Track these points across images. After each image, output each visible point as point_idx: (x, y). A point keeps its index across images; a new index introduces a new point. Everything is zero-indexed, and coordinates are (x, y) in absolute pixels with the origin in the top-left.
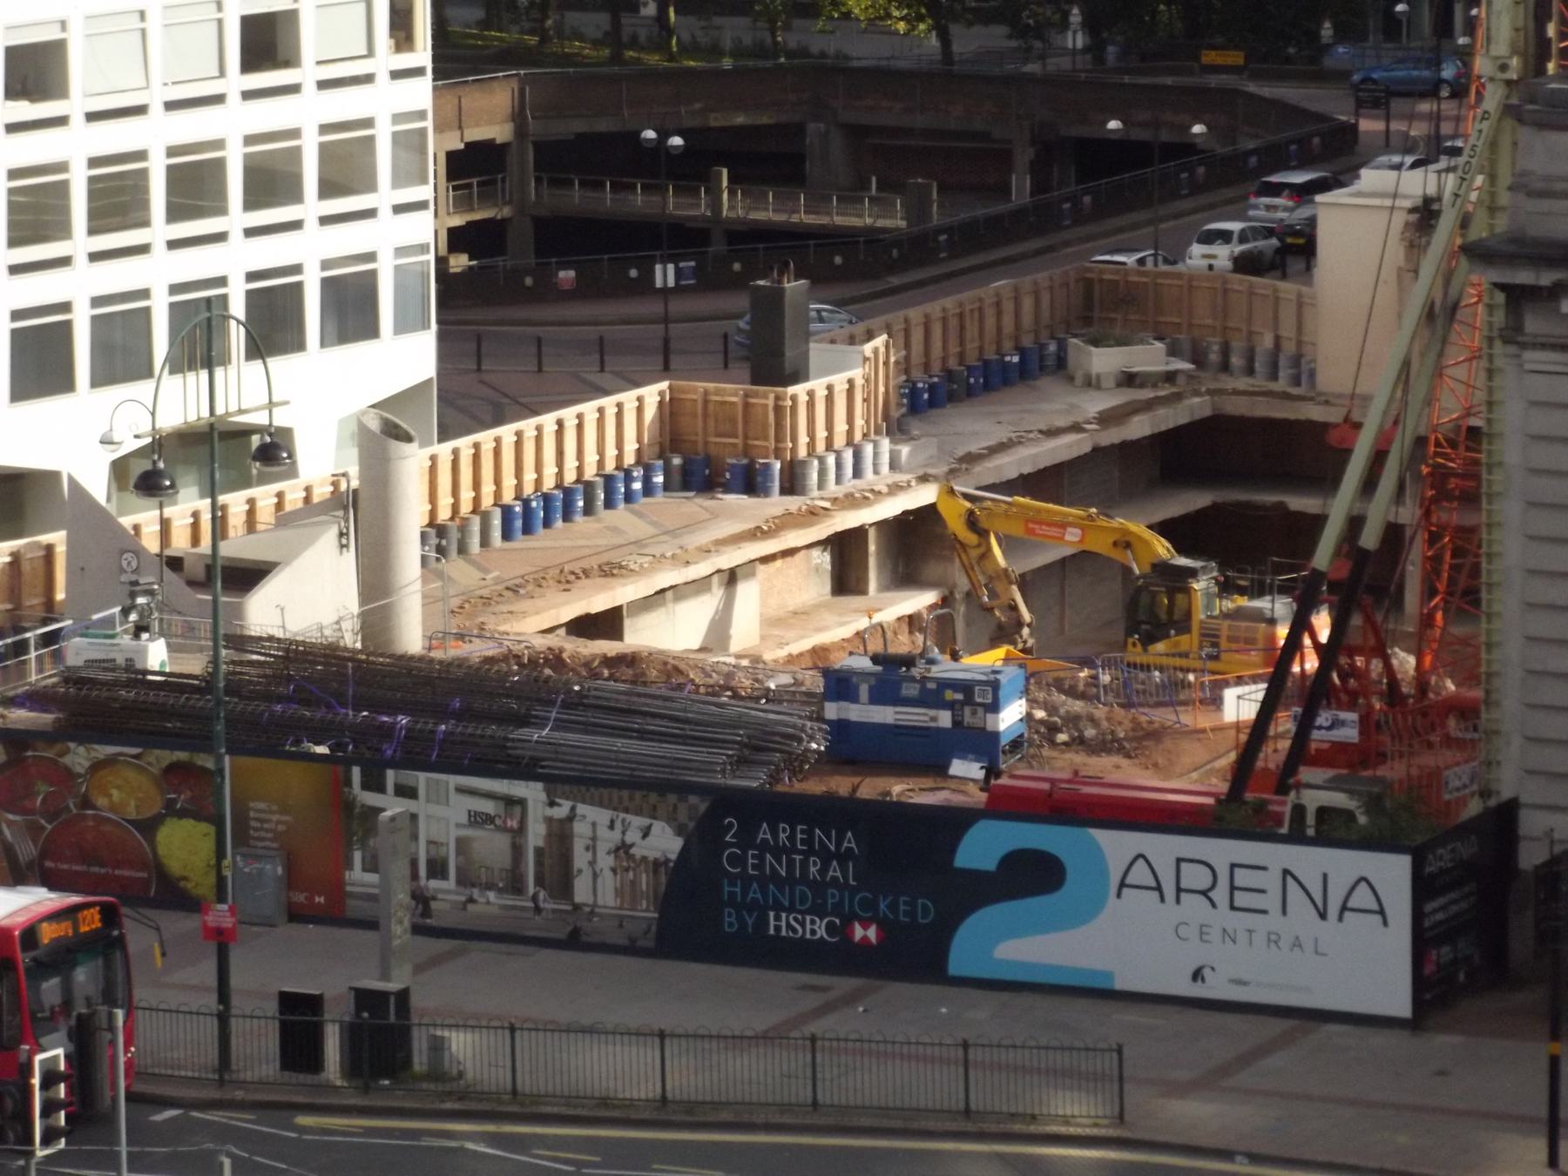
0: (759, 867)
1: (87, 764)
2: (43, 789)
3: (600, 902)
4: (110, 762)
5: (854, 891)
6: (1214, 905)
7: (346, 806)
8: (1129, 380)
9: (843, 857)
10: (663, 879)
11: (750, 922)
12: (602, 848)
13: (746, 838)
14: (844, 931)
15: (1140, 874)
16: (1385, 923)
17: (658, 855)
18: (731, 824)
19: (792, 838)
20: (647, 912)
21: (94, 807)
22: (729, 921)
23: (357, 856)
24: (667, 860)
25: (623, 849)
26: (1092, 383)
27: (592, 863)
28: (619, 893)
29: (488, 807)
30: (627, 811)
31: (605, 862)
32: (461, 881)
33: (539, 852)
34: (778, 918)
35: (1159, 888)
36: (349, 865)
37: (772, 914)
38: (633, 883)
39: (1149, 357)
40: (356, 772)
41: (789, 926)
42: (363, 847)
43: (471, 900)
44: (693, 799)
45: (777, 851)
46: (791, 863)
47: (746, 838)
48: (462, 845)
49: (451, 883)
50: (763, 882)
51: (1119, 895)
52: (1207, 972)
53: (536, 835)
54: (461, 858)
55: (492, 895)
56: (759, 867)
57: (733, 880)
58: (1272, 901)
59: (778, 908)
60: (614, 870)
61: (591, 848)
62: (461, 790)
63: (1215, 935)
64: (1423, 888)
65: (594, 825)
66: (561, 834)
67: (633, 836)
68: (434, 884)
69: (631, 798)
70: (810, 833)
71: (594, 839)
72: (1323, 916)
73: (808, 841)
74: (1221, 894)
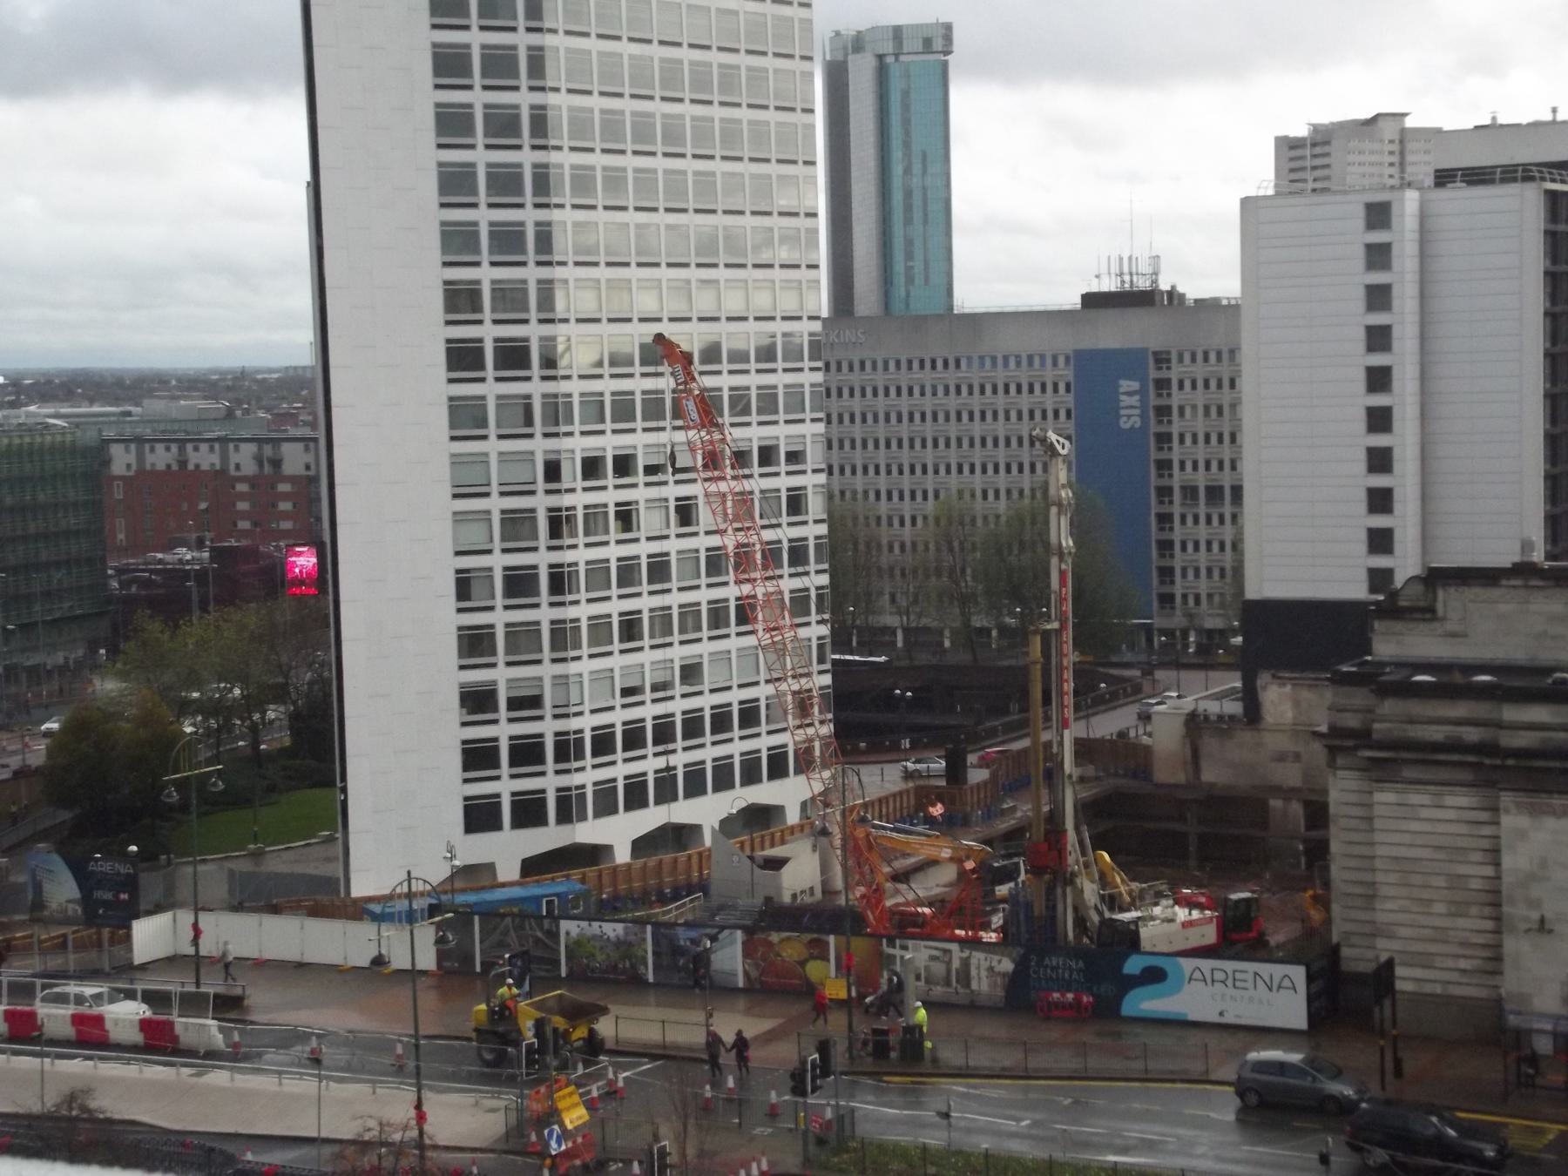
2: (761, 950)
4: (788, 939)
7: (881, 954)
15: (1197, 975)
20: (1000, 993)
25: (991, 969)
28: (989, 986)
31: (984, 974)
32: (928, 981)
33: (957, 973)
35: (1205, 980)
40: (884, 941)
48: (927, 968)
53: (956, 964)
55: (939, 988)
58: (1250, 985)
61: (978, 968)
62: (926, 947)
64: (1310, 979)
66: (966, 963)
72: (1270, 989)
74: (1230, 983)
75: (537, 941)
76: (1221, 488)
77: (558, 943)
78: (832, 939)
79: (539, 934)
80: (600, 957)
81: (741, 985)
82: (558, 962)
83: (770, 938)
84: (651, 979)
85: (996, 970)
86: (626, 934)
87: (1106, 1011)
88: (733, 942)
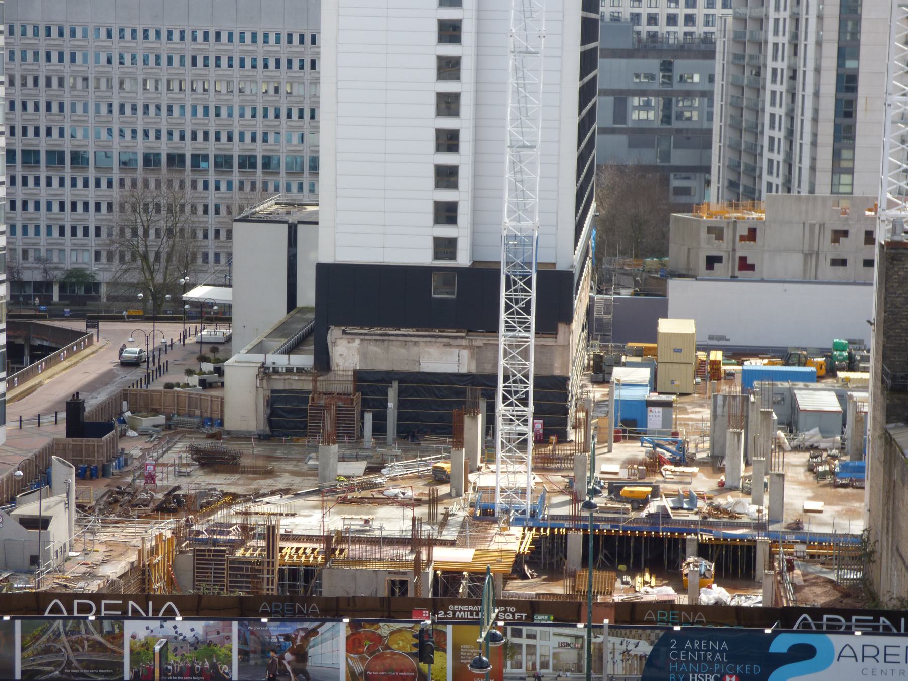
0: (686, 657)
1: (388, 632)
3: (616, 673)
4: (399, 630)
6: (878, 661)
9: (722, 652)
10: (644, 662)
12: (617, 653)
13: (680, 647)
17: (641, 653)
18: (674, 642)
19: (700, 645)
23: (509, 663)
24: (646, 655)
25: (626, 652)
27: (613, 658)
29: (568, 640)
31: (619, 657)
34: (693, 676)
35: (855, 656)
36: (505, 667)
37: (691, 675)
43: (559, 676)
44: (657, 631)
46: (699, 656)
47: (680, 647)
48: (554, 654)
49: (551, 670)
51: (838, 660)
54: (555, 661)
55: (568, 674)
56: (686, 657)
59: (694, 672)
60: (622, 661)
61: (613, 653)
62: (555, 634)
63: (878, 672)
65: (614, 644)
68: (543, 671)
69: (630, 632)
70: (708, 643)
71: (614, 649)
73: (707, 646)
74: (881, 657)
75: (96, 646)
76: (37, 153)
77: (121, 646)
78: (449, 629)
79: (98, 637)
82: (121, 665)
83: (379, 631)
86: (207, 634)
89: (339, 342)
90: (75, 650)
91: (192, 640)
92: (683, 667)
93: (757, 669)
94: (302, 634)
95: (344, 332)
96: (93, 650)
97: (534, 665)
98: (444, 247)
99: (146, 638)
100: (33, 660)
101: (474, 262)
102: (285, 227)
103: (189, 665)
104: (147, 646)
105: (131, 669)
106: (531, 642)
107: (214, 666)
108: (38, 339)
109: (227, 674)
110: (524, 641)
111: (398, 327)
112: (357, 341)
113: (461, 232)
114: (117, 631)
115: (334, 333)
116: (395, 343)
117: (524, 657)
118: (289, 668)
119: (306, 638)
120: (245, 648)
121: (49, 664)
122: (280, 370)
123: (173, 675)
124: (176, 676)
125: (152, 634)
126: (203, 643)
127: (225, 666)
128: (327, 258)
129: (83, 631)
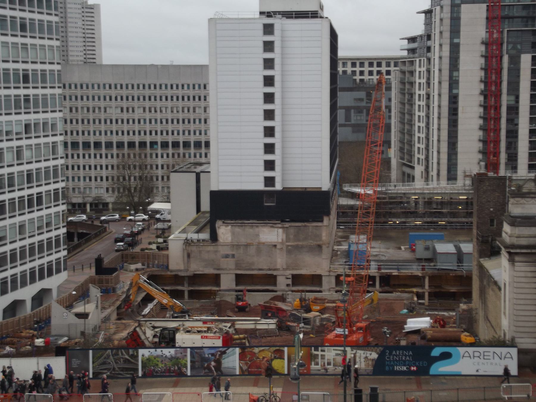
2: (249, 356)
4: (263, 350)
5: (411, 361)
7: (311, 355)
8: (137, 270)
10: (374, 362)
11: (391, 368)
13: (390, 354)
14: (409, 369)
16: (513, 359)
20: (371, 368)
21: (259, 358)
22: (387, 368)
23: (313, 363)
26: (131, 271)
28: (365, 365)
29: (339, 352)
30: (367, 351)
31: (363, 360)
32: (334, 365)
35: (470, 357)
36: (311, 364)
38: (368, 363)
39: (139, 266)
41: (399, 368)
42: (314, 361)
43: (336, 369)
44: (380, 348)
45: (396, 356)
46: (399, 358)
47: (390, 354)
48: (334, 359)
49: (332, 366)
50: (393, 361)
52: (479, 370)
57: (388, 361)
58: (491, 357)
59: (397, 365)
61: (360, 358)
62: (334, 350)
67: (368, 355)
68: (329, 367)
70: (403, 352)
71: (360, 356)
72: (501, 359)
74: (482, 357)
75: (126, 361)
77: (137, 361)
78: (286, 349)
79: (127, 357)
80: (160, 365)
81: (238, 373)
82: (137, 370)
83: (254, 351)
84: (189, 373)
85: (369, 358)
86: (176, 354)
87: (424, 371)
88: (235, 353)
89: (221, 227)
90: (116, 363)
91: (169, 357)
92: (392, 363)
93: (425, 364)
94: (219, 353)
95: (224, 223)
96: (125, 363)
97: (324, 363)
98: (270, 181)
99: (149, 356)
100: (98, 368)
101: (284, 188)
102: (194, 174)
103: (168, 368)
104: (149, 359)
105: (142, 370)
106: (323, 353)
107: (179, 369)
108: (81, 229)
109: (185, 372)
110: (319, 353)
111: (248, 219)
112: (229, 227)
113: (276, 174)
114: (136, 354)
115: (219, 223)
116: (248, 227)
117: (320, 360)
118: (213, 369)
119: (221, 356)
120: (194, 360)
121: (105, 369)
122: (194, 241)
123: (161, 373)
124: (162, 373)
125: (152, 354)
126: (174, 358)
127: (185, 369)
128: (214, 188)
129: (120, 354)
